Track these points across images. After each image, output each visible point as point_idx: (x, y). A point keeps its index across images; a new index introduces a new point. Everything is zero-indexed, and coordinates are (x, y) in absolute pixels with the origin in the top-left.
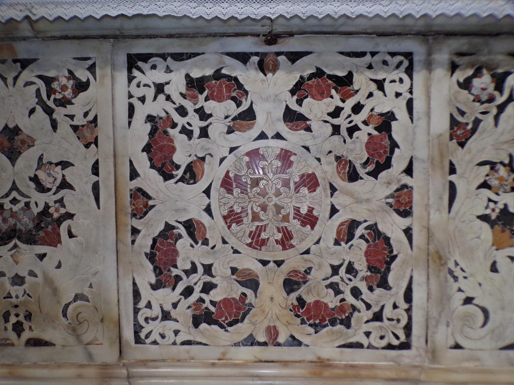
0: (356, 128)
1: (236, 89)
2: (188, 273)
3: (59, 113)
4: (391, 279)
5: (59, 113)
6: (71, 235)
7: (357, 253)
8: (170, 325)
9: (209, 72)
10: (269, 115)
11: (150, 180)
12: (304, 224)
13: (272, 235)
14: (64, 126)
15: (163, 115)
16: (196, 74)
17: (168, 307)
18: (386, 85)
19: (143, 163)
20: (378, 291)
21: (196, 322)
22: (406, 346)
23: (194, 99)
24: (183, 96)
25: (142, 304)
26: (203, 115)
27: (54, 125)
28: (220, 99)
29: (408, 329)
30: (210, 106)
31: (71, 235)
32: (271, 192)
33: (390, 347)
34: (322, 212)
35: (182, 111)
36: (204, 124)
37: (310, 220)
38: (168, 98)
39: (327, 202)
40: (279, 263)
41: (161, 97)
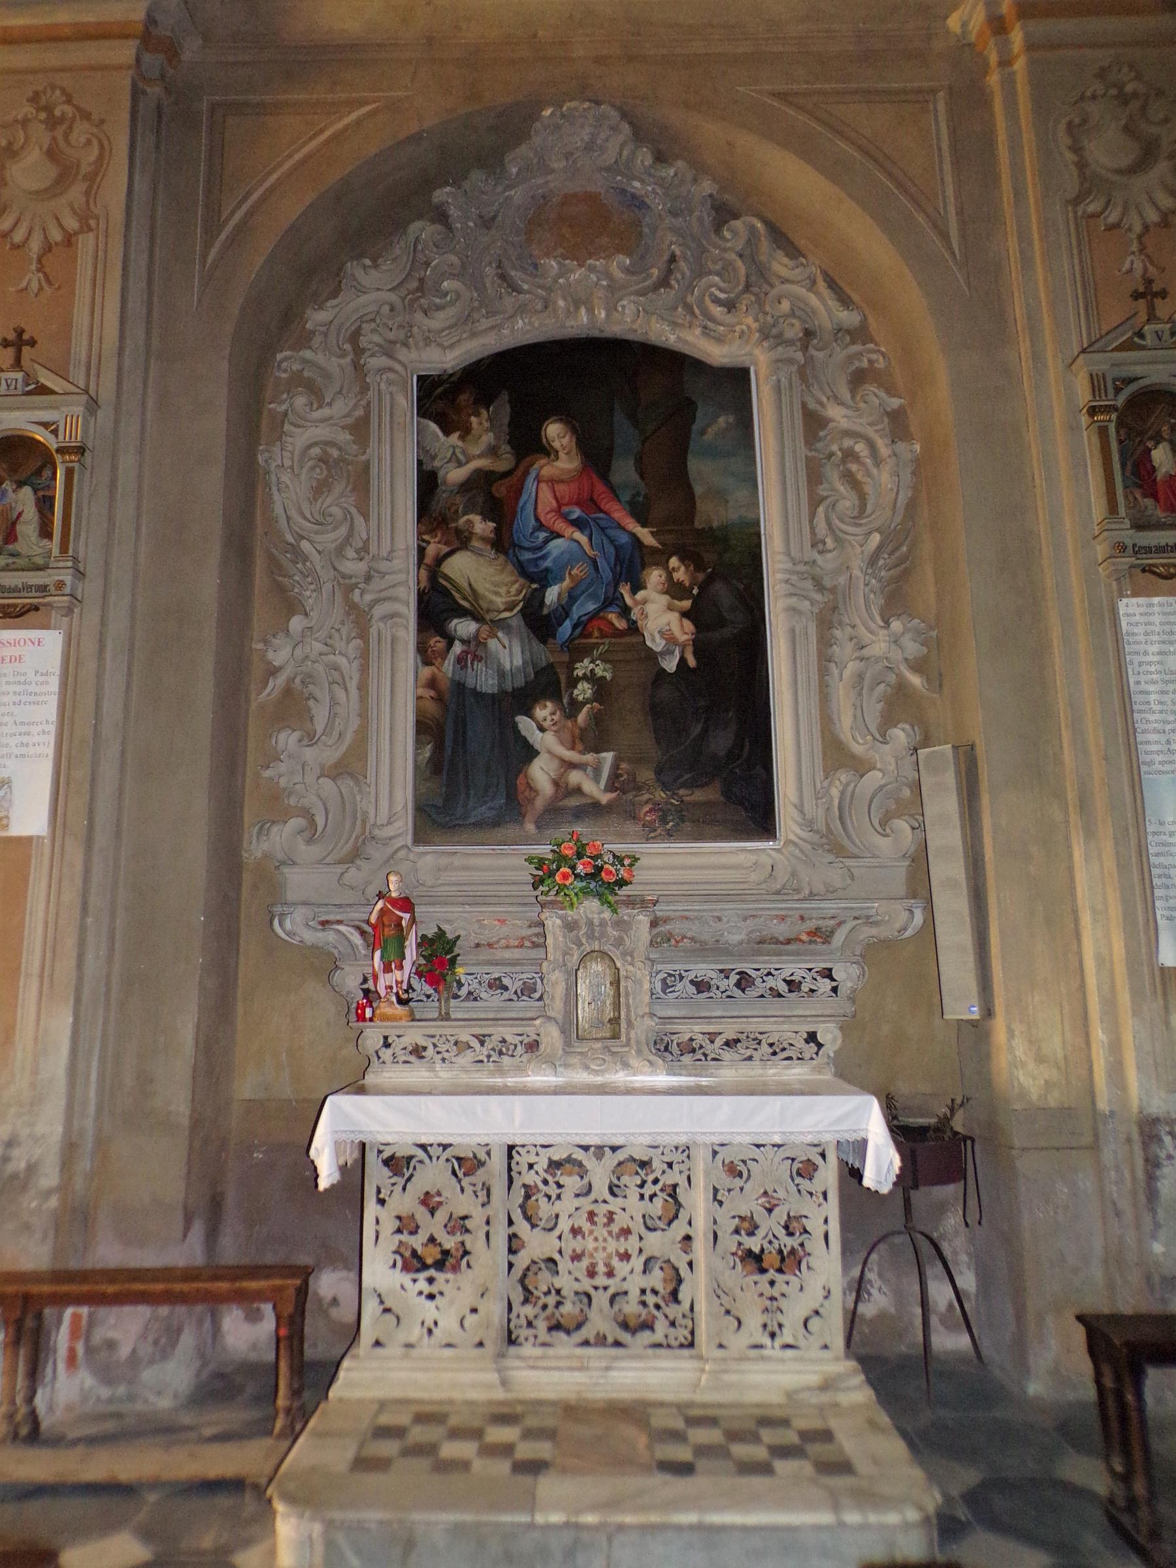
0: (655, 1195)
1: (580, 1169)
2: (546, 1294)
3: (466, 1182)
4: (681, 1296)
5: (466, 1182)
6: (469, 1266)
7: (656, 1278)
8: (531, 1332)
9: (564, 1156)
10: (601, 1189)
11: (522, 1227)
12: (621, 1260)
13: (601, 1269)
14: (469, 1190)
15: (532, 1184)
16: (556, 1158)
17: (531, 1317)
18: (675, 1166)
19: (517, 1216)
20: (674, 1306)
21: (551, 1329)
22: (691, 1345)
23: (554, 1175)
24: (546, 1171)
25: (513, 1316)
26: (559, 1186)
27: (462, 1190)
28: (570, 1174)
29: (692, 1333)
30: (563, 1180)
31: (469, 1266)
32: (601, 1239)
33: (682, 1346)
34: (634, 1252)
35: (546, 1182)
36: (558, 1191)
37: (626, 1257)
38: (537, 1173)
39: (637, 1245)
40: (605, 1288)
41: (532, 1172)
